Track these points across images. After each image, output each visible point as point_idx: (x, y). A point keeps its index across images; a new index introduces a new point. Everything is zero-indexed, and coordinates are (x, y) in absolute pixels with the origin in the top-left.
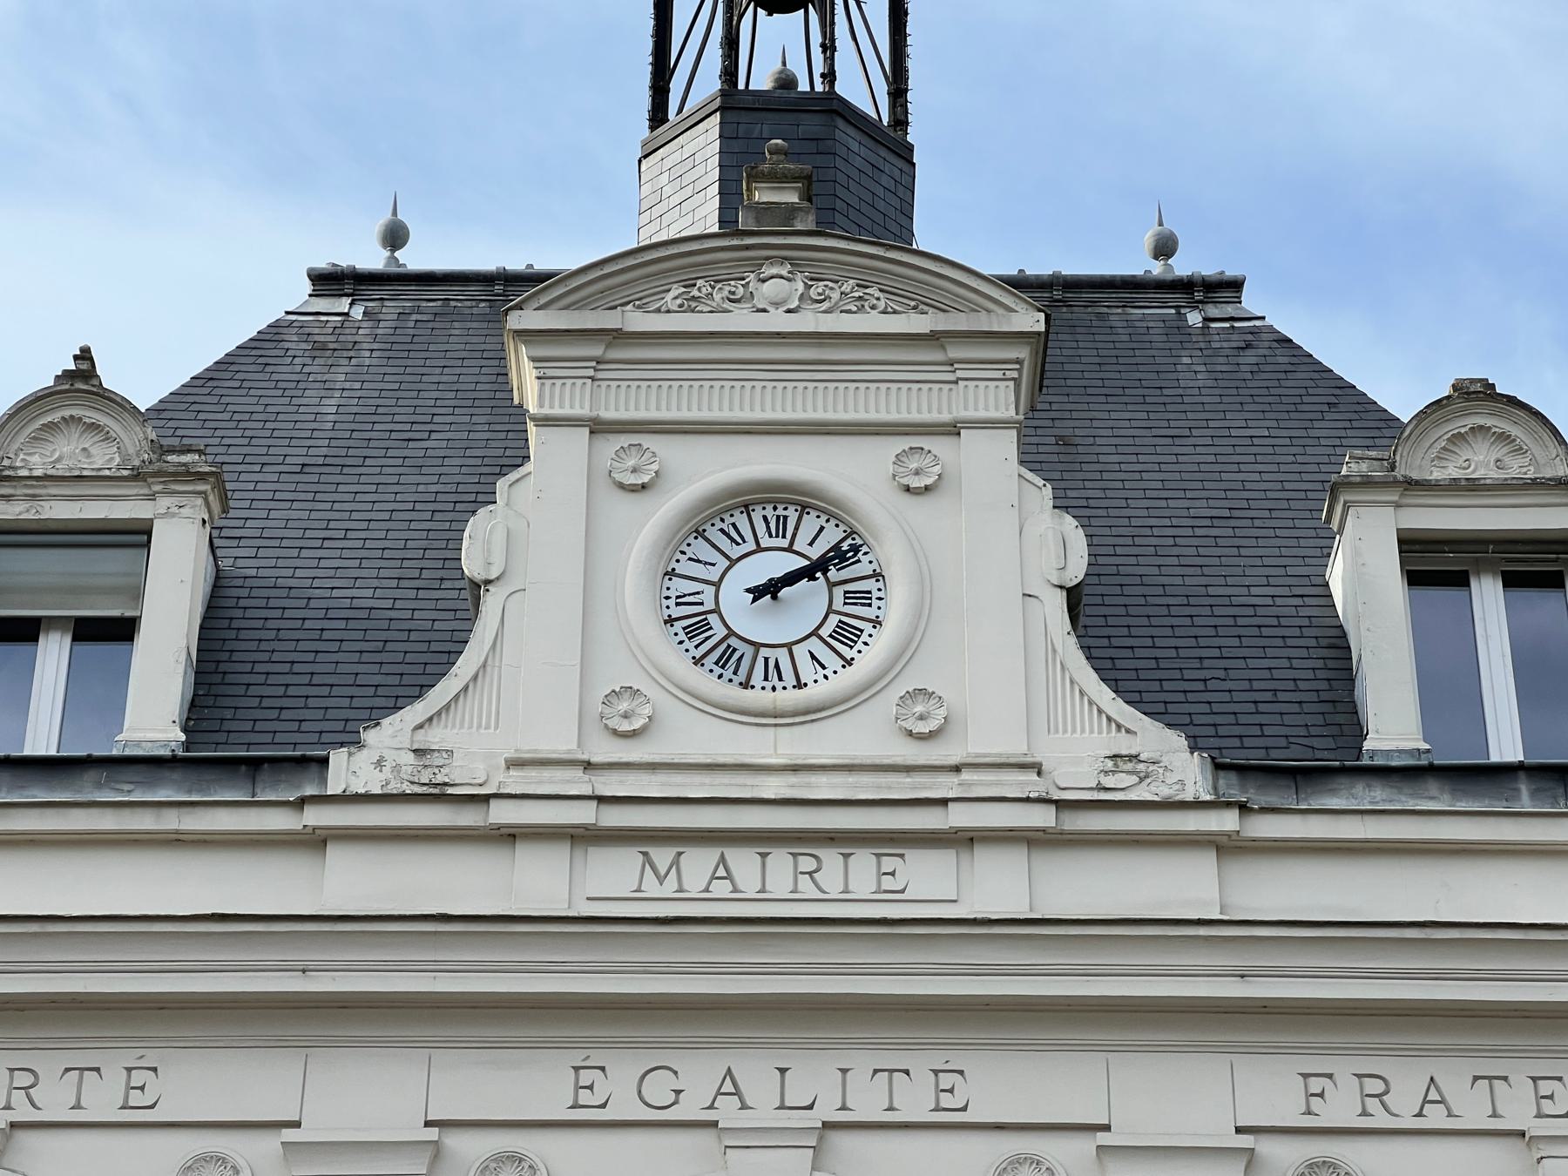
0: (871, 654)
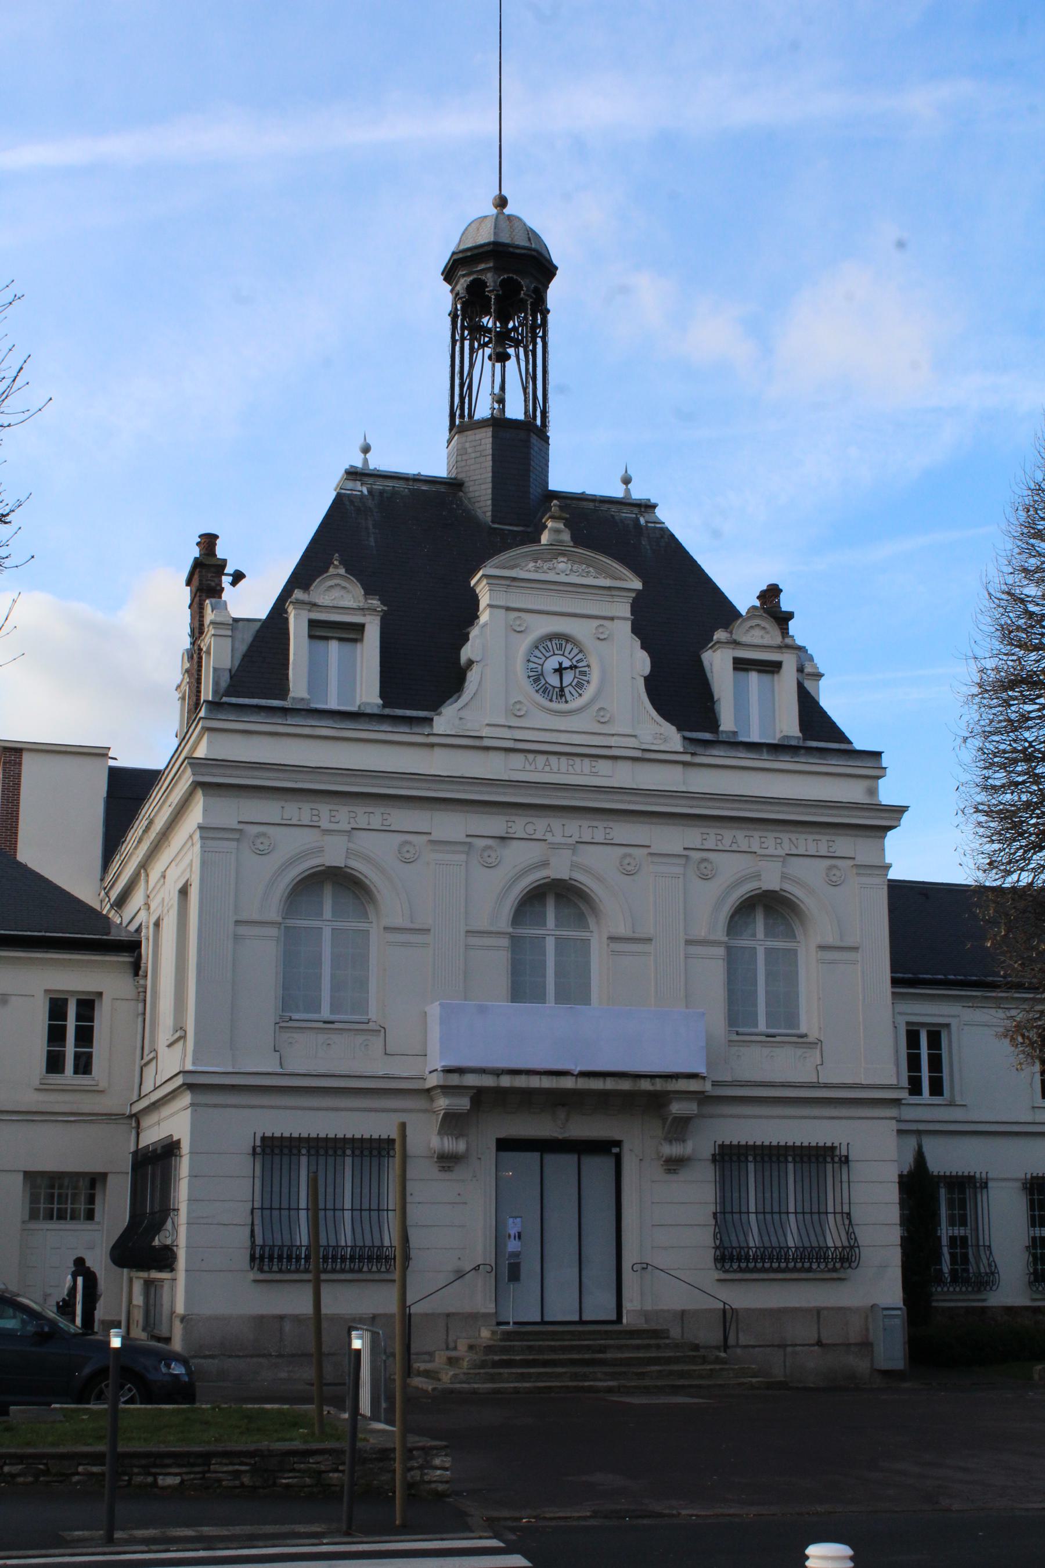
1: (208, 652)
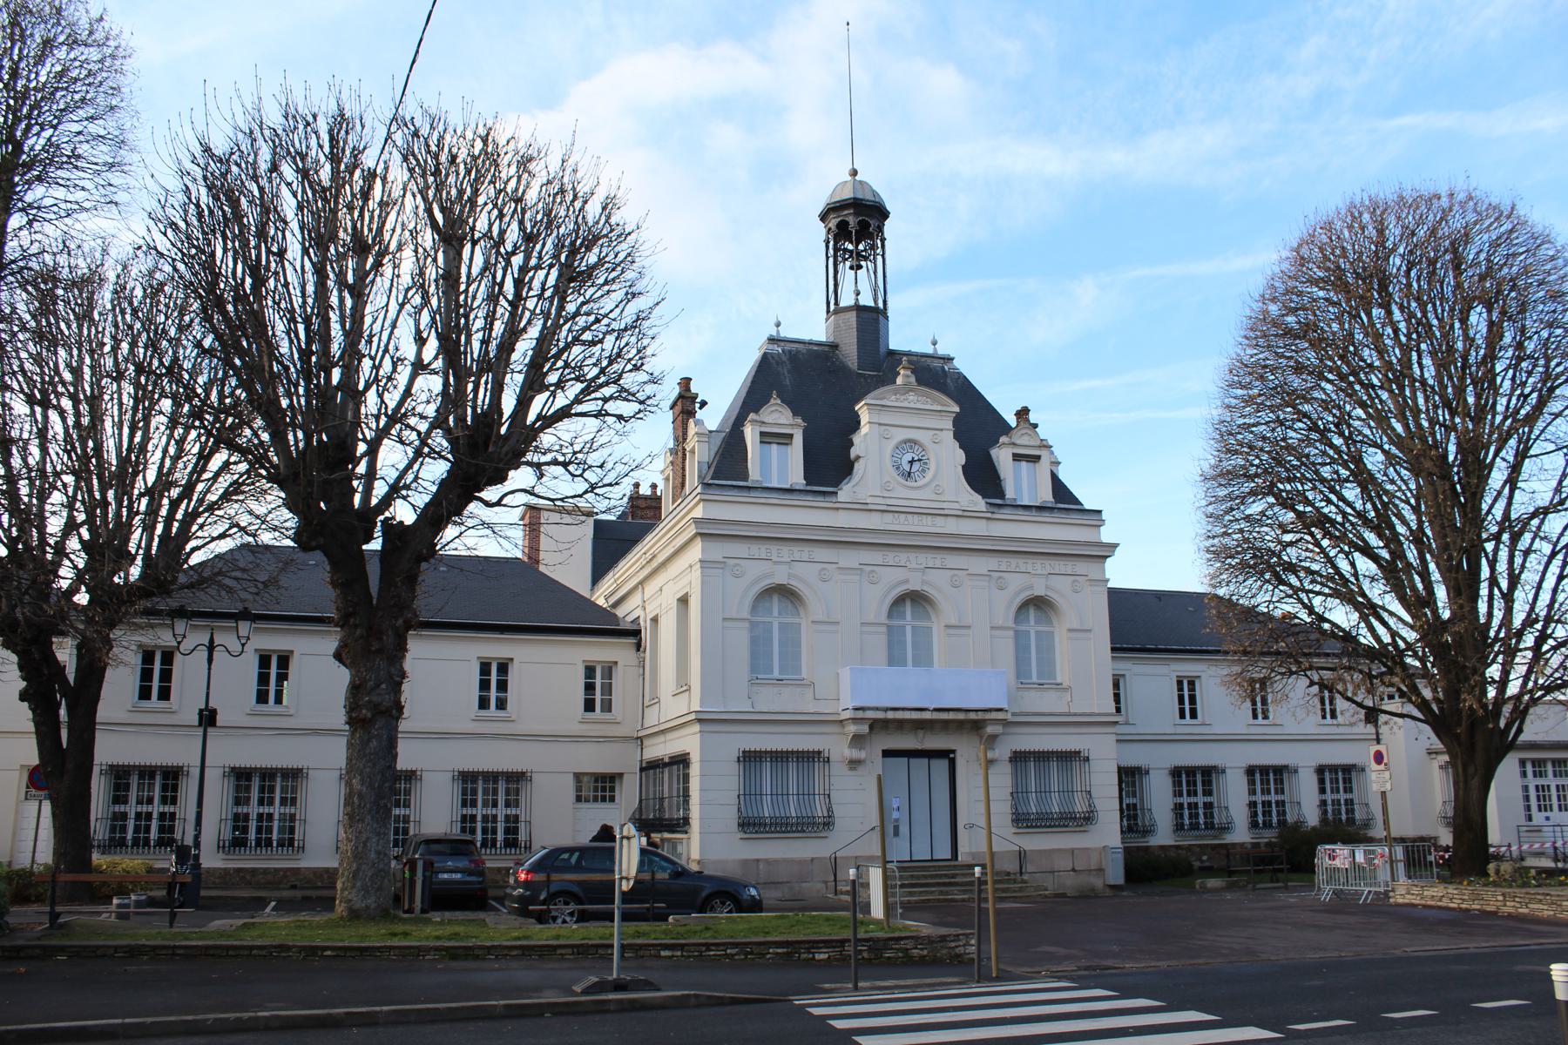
0: (929, 475)
1: (692, 451)
